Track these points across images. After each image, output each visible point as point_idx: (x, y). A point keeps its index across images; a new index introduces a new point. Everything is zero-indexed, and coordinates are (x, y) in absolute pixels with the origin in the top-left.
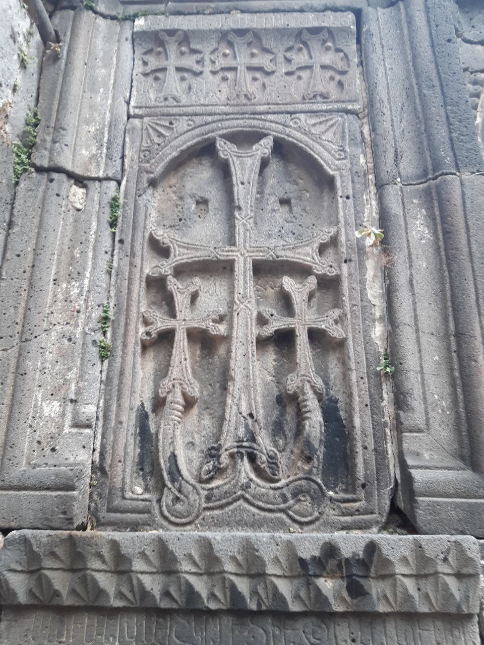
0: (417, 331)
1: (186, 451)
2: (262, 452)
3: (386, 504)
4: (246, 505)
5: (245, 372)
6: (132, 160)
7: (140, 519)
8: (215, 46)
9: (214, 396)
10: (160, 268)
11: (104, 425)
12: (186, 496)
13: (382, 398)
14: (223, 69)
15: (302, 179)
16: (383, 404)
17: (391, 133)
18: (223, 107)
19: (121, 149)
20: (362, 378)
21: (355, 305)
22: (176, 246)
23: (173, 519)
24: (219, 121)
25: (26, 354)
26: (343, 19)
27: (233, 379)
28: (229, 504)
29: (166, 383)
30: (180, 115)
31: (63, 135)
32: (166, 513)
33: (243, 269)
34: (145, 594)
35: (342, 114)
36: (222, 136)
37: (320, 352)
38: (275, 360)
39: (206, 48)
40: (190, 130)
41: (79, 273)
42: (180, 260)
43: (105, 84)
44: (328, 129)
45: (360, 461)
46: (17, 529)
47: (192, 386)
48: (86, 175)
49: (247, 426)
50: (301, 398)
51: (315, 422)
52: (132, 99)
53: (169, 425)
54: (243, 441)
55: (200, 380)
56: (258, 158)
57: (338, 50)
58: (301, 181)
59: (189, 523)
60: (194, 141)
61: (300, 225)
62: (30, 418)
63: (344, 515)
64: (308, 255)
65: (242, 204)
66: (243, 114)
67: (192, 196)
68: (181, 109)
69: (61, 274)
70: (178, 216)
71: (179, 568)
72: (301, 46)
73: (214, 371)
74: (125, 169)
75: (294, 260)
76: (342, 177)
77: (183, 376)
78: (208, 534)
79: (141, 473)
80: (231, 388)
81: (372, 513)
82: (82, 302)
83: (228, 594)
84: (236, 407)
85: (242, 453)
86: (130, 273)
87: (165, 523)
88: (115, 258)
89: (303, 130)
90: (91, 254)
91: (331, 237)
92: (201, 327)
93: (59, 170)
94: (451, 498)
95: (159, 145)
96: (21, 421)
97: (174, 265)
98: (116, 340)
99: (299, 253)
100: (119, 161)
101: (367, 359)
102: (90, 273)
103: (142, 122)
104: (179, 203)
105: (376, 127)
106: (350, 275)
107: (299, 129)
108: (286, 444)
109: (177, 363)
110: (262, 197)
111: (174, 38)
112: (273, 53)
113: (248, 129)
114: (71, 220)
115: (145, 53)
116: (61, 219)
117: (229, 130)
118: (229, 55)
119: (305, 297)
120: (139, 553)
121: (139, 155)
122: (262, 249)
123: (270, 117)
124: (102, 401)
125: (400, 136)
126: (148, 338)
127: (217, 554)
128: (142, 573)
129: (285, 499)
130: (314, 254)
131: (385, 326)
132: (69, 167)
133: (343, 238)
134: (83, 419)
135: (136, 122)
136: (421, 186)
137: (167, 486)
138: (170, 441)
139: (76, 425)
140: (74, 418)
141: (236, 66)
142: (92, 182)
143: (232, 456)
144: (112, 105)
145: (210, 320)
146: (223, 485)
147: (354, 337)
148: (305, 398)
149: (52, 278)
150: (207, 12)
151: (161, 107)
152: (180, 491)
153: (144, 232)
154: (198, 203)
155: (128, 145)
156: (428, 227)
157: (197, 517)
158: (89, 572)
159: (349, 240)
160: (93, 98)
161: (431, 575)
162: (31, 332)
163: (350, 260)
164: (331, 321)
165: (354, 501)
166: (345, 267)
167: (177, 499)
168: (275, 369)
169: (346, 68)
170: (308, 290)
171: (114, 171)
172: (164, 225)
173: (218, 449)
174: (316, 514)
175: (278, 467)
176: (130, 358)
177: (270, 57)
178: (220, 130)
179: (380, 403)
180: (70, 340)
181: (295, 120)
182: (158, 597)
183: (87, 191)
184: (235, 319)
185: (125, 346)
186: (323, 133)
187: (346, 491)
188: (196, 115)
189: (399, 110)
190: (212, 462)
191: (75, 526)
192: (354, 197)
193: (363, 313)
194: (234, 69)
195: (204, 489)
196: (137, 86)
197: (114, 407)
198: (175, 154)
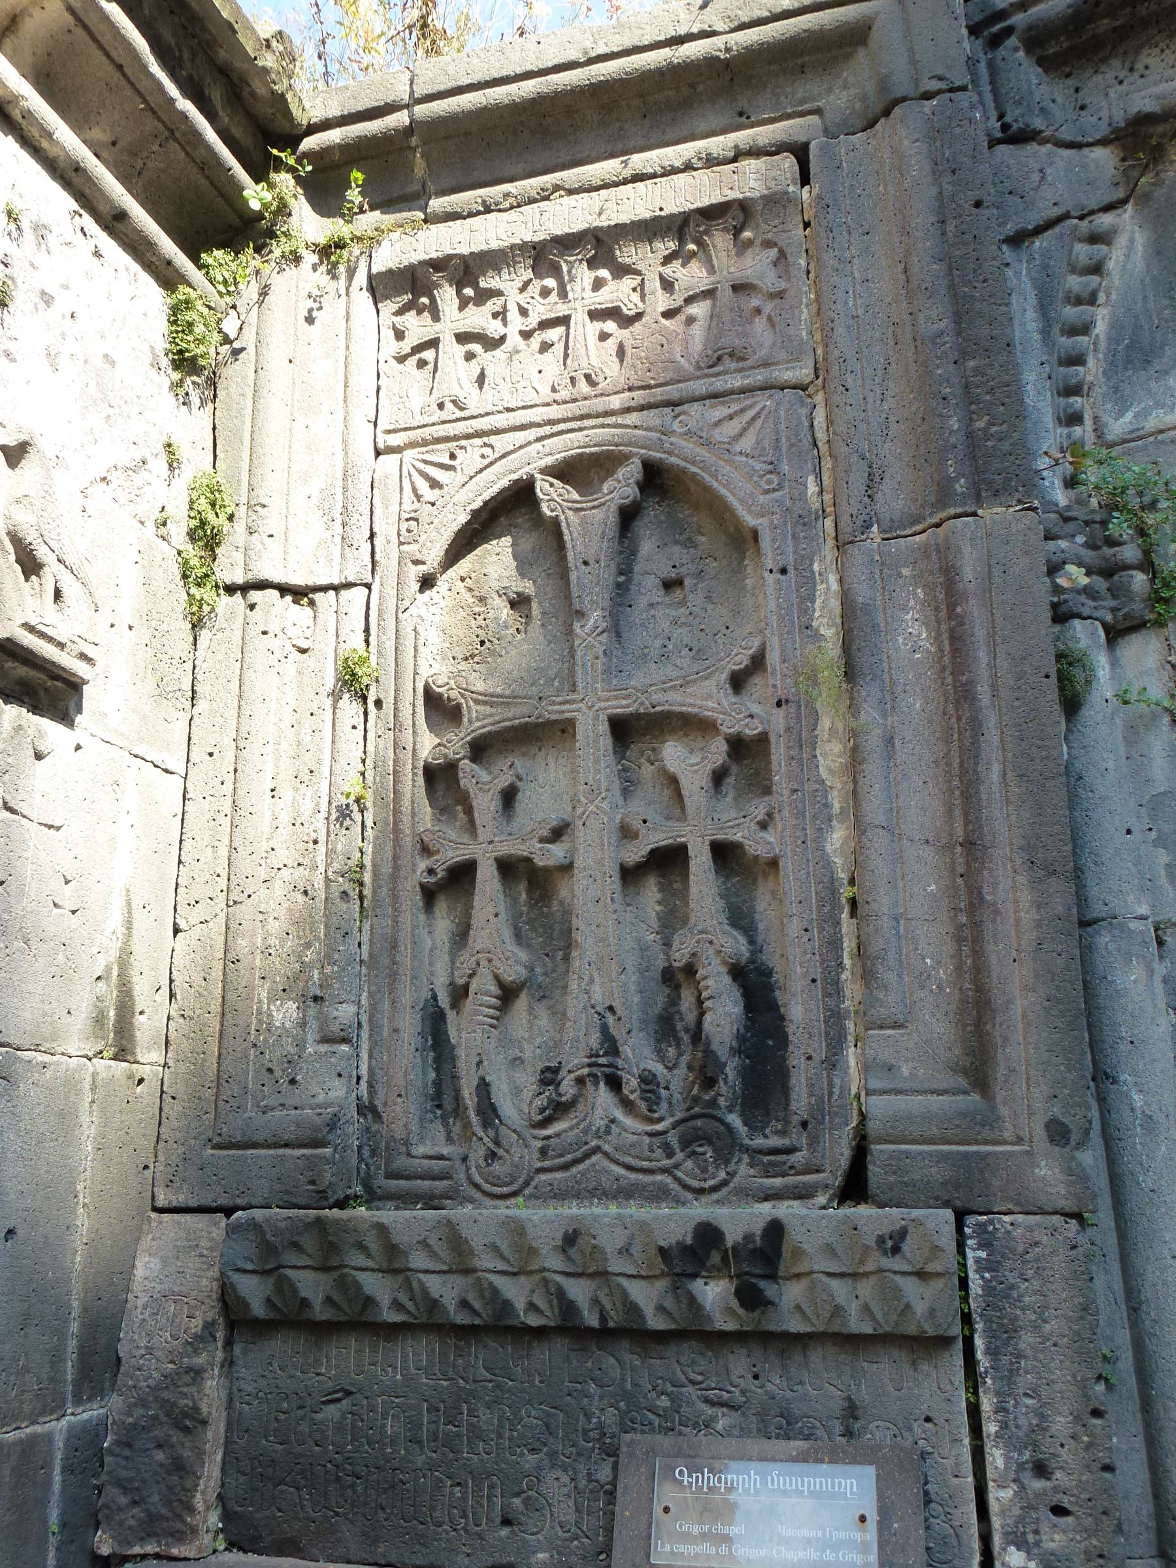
3: (842, 1154)
4: (606, 1163)
6: (388, 542)
7: (436, 1188)
10: (445, 746)
11: (371, 1036)
12: (507, 1151)
13: (841, 965)
14: (544, 325)
16: (844, 977)
20: (806, 930)
22: (471, 703)
23: (487, 1187)
24: (539, 439)
29: (466, 960)
30: (468, 437)
32: (478, 1179)
34: (434, 1305)
38: (659, 903)
42: (480, 728)
44: (745, 430)
46: (244, 1209)
47: (509, 962)
49: (604, 1029)
54: (598, 1056)
56: (613, 508)
57: (768, 244)
59: (514, 1194)
62: (253, 1032)
64: (709, 696)
66: (582, 417)
71: (478, 1263)
72: (692, 247)
73: (551, 928)
78: (523, 1213)
79: (439, 1112)
81: (818, 1171)
83: (555, 1302)
84: (586, 996)
85: (595, 1076)
87: (478, 1195)
94: (934, 1144)
97: (468, 738)
98: (380, 887)
99: (692, 695)
104: (477, 609)
105: (833, 417)
108: (680, 1055)
109: (483, 923)
110: (629, 580)
112: (638, 273)
113: (593, 450)
117: (558, 456)
124: (365, 994)
126: (432, 880)
127: (535, 1244)
128: (426, 1272)
129: (670, 1154)
133: (773, 658)
134: (335, 1028)
135: (390, 461)
139: (325, 1040)
140: (321, 1029)
141: (566, 313)
143: (580, 1081)
145: (536, 840)
146: (565, 1131)
150: (506, 205)
152: (497, 1143)
156: (927, 625)
157: (527, 1184)
158: (346, 1270)
159: (784, 661)
161: (872, 1273)
162: (240, 888)
164: (754, 827)
167: (492, 1156)
168: (659, 919)
169: (783, 285)
170: (709, 768)
171: (358, 569)
173: (556, 1071)
174: (722, 1175)
176: (406, 920)
179: (838, 974)
180: (306, 893)
182: (451, 1308)
183: (315, 612)
187: (783, 1133)
188: (497, 432)
189: (880, 372)
190: (547, 1093)
191: (331, 1201)
192: (796, 569)
194: (564, 321)
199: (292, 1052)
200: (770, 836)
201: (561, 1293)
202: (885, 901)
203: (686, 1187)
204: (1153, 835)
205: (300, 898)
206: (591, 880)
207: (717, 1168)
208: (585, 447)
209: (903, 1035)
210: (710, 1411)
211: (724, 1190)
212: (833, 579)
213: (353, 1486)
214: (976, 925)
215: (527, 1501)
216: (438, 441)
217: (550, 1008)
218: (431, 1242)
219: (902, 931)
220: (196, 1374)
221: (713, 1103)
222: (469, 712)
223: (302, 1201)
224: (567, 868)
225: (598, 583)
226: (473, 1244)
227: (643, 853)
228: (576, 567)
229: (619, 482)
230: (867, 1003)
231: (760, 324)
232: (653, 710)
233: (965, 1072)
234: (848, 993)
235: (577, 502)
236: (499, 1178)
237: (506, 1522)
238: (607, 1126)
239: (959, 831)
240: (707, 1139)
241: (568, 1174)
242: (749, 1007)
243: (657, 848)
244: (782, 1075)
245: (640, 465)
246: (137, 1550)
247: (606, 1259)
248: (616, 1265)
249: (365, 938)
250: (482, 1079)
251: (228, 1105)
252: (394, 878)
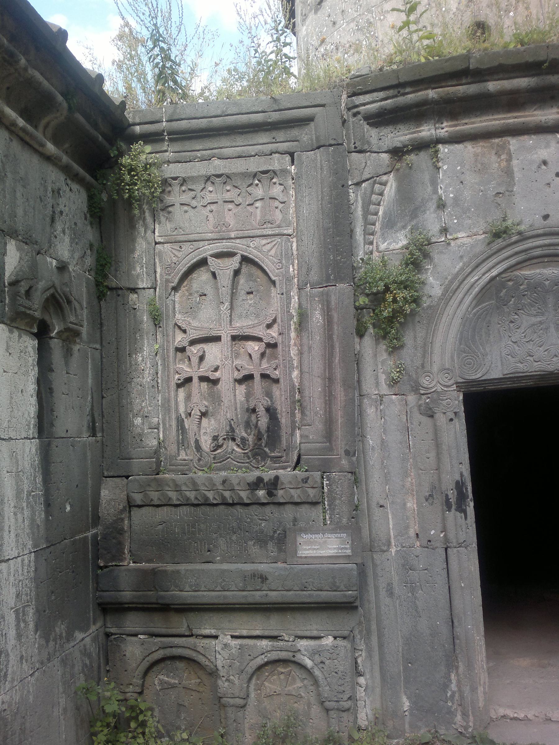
8: (203, 186)
23: (198, 468)
28: (224, 461)
30: (186, 241)
32: (196, 466)
33: (226, 339)
34: (188, 499)
36: (212, 256)
39: (198, 187)
49: (231, 425)
51: (264, 421)
56: (232, 270)
64: (261, 331)
67: (197, 292)
72: (257, 182)
75: (253, 334)
106: (282, 342)
107: (255, 248)
126: (180, 382)
129: (249, 458)
133: (279, 320)
134: (153, 425)
140: (149, 425)
150: (196, 160)
165: (281, 457)
166: (280, 337)
169: (286, 199)
174: (263, 463)
176: (173, 394)
180: (141, 386)
185: (169, 387)
186: (269, 251)
187: (279, 452)
194: (217, 202)
198: (185, 269)
200: (277, 372)
201: (222, 495)
202: (307, 393)
203: (254, 467)
204: (382, 370)
210: (260, 522)
212: (296, 298)
213: (167, 545)
214: (330, 400)
215: (214, 546)
220: (122, 520)
221: (261, 445)
230: (302, 419)
231: (278, 212)
233: (326, 438)
234: (297, 416)
237: (209, 551)
239: (327, 375)
242: (270, 419)
244: (279, 437)
246: (110, 564)
248: (236, 488)
250: (196, 439)
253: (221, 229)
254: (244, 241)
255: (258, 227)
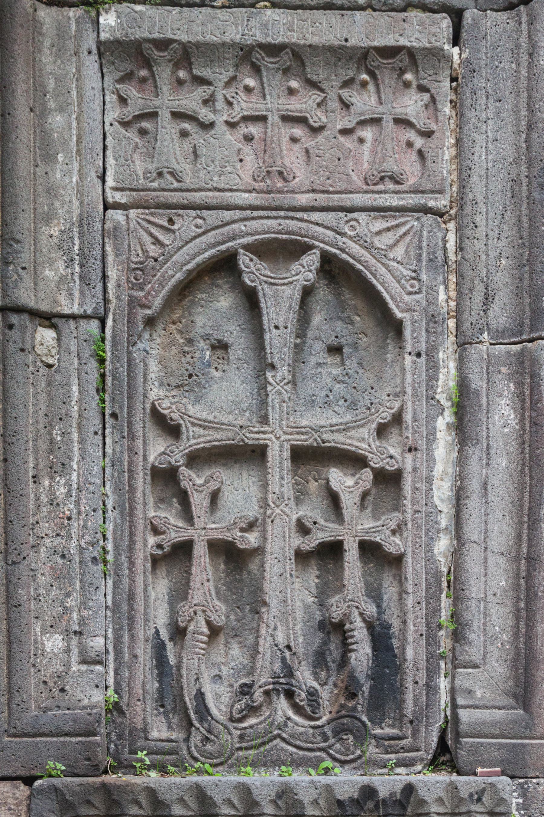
0: (486, 549)
1: (213, 685)
2: (300, 689)
3: (433, 741)
4: (283, 745)
5: (281, 596)
6: (119, 286)
8: (231, 73)
9: (244, 621)
10: (169, 455)
11: (115, 660)
12: (216, 737)
15: (359, 316)
17: (484, 257)
18: (246, 195)
19: (100, 266)
21: (418, 511)
22: (189, 425)
25: (16, 580)
26: (434, 29)
27: (265, 604)
28: (263, 744)
30: (184, 207)
31: (18, 252)
32: (196, 754)
35: (420, 214)
36: (247, 248)
37: (372, 567)
40: (200, 235)
41: (63, 464)
42: (195, 444)
43: (65, 143)
44: (398, 241)
45: (409, 697)
47: (218, 613)
48: (55, 311)
49: (284, 660)
50: (347, 626)
52: (108, 173)
53: (193, 659)
54: (279, 677)
55: (225, 601)
56: (299, 287)
57: (422, 89)
58: (358, 319)
59: (221, 764)
60: (207, 255)
61: (354, 388)
63: (387, 753)
64: (363, 440)
65: (276, 361)
68: (185, 194)
69: (41, 467)
70: (187, 370)
74: (109, 301)
75: (345, 447)
76: (414, 322)
77: (207, 601)
79: (162, 710)
80: (265, 616)
81: (418, 750)
82: (72, 506)
85: (278, 690)
86: (130, 463)
88: (108, 440)
89: (362, 242)
90: (76, 435)
91: (394, 415)
92: (226, 538)
93: (19, 310)
95: (156, 260)
96: (23, 661)
97: (187, 451)
98: (120, 555)
99: (351, 438)
100: (100, 285)
101: (426, 580)
102: (78, 463)
103: (127, 216)
105: (464, 246)
106: (415, 469)
109: (198, 585)
111: (166, 54)
112: (322, 90)
113: (284, 237)
114: (43, 384)
115: (121, 80)
116: (30, 386)
117: (257, 237)
118: (254, 89)
119: (357, 500)
120: (178, 799)
121: (128, 278)
122: (303, 430)
123: (316, 216)
124: (110, 631)
125: (494, 263)
126: (160, 552)
129: (326, 740)
130: (371, 440)
131: (451, 539)
132: (32, 304)
133: (408, 417)
135: (117, 215)
136: (513, 347)
137: (195, 726)
138: (195, 677)
139: (85, 661)
141: (265, 113)
142: (64, 320)
143: (267, 693)
144: (80, 186)
145: (237, 530)
146: (257, 724)
147: (414, 553)
148: (352, 627)
149: (31, 474)
151: (155, 190)
152: (209, 732)
153: (144, 401)
154: (213, 347)
155: (110, 258)
157: (229, 758)
159: (416, 421)
160: (50, 173)
163: (416, 449)
164: (388, 532)
165: (400, 738)
166: (409, 457)
170: (361, 490)
172: (169, 385)
173: (250, 686)
174: (359, 752)
175: (319, 705)
176: (140, 580)
177: (317, 96)
178: (243, 237)
181: (353, 223)
184: (269, 528)
185: (132, 563)
190: (244, 701)
192: (427, 355)
193: (427, 522)
194: (263, 119)
195: (236, 728)
196: (114, 148)
197: (126, 639)
198: (179, 276)
199: (61, 670)
205: (60, 561)
206: (277, 560)
207: (356, 748)
208: (278, 233)
209: (479, 672)
211: (359, 761)
212: (452, 365)
216: (158, 206)
217: (240, 643)
218: (186, 798)
219: (482, 609)
221: (354, 709)
222: (187, 431)
223: (82, 772)
224: (259, 551)
225: (285, 345)
226: (215, 799)
227: (313, 545)
228: (270, 330)
229: (304, 267)
232: (323, 445)
234: (442, 644)
235: (271, 278)
236: (211, 754)
238: (285, 722)
240: (348, 730)
241: (259, 751)
243: (323, 542)
245: (319, 256)
247: (304, 807)
249: (110, 591)
251: (20, 707)
252: (131, 548)
253: (274, 184)
254: (328, 218)
255: (365, 187)
